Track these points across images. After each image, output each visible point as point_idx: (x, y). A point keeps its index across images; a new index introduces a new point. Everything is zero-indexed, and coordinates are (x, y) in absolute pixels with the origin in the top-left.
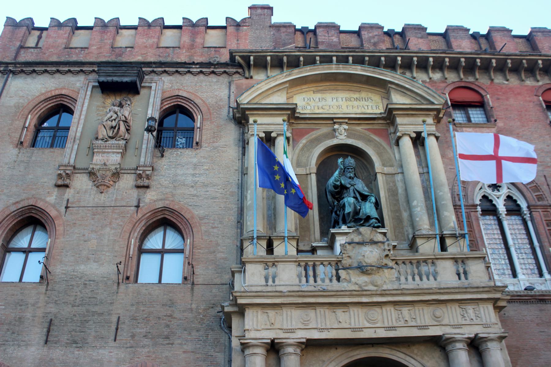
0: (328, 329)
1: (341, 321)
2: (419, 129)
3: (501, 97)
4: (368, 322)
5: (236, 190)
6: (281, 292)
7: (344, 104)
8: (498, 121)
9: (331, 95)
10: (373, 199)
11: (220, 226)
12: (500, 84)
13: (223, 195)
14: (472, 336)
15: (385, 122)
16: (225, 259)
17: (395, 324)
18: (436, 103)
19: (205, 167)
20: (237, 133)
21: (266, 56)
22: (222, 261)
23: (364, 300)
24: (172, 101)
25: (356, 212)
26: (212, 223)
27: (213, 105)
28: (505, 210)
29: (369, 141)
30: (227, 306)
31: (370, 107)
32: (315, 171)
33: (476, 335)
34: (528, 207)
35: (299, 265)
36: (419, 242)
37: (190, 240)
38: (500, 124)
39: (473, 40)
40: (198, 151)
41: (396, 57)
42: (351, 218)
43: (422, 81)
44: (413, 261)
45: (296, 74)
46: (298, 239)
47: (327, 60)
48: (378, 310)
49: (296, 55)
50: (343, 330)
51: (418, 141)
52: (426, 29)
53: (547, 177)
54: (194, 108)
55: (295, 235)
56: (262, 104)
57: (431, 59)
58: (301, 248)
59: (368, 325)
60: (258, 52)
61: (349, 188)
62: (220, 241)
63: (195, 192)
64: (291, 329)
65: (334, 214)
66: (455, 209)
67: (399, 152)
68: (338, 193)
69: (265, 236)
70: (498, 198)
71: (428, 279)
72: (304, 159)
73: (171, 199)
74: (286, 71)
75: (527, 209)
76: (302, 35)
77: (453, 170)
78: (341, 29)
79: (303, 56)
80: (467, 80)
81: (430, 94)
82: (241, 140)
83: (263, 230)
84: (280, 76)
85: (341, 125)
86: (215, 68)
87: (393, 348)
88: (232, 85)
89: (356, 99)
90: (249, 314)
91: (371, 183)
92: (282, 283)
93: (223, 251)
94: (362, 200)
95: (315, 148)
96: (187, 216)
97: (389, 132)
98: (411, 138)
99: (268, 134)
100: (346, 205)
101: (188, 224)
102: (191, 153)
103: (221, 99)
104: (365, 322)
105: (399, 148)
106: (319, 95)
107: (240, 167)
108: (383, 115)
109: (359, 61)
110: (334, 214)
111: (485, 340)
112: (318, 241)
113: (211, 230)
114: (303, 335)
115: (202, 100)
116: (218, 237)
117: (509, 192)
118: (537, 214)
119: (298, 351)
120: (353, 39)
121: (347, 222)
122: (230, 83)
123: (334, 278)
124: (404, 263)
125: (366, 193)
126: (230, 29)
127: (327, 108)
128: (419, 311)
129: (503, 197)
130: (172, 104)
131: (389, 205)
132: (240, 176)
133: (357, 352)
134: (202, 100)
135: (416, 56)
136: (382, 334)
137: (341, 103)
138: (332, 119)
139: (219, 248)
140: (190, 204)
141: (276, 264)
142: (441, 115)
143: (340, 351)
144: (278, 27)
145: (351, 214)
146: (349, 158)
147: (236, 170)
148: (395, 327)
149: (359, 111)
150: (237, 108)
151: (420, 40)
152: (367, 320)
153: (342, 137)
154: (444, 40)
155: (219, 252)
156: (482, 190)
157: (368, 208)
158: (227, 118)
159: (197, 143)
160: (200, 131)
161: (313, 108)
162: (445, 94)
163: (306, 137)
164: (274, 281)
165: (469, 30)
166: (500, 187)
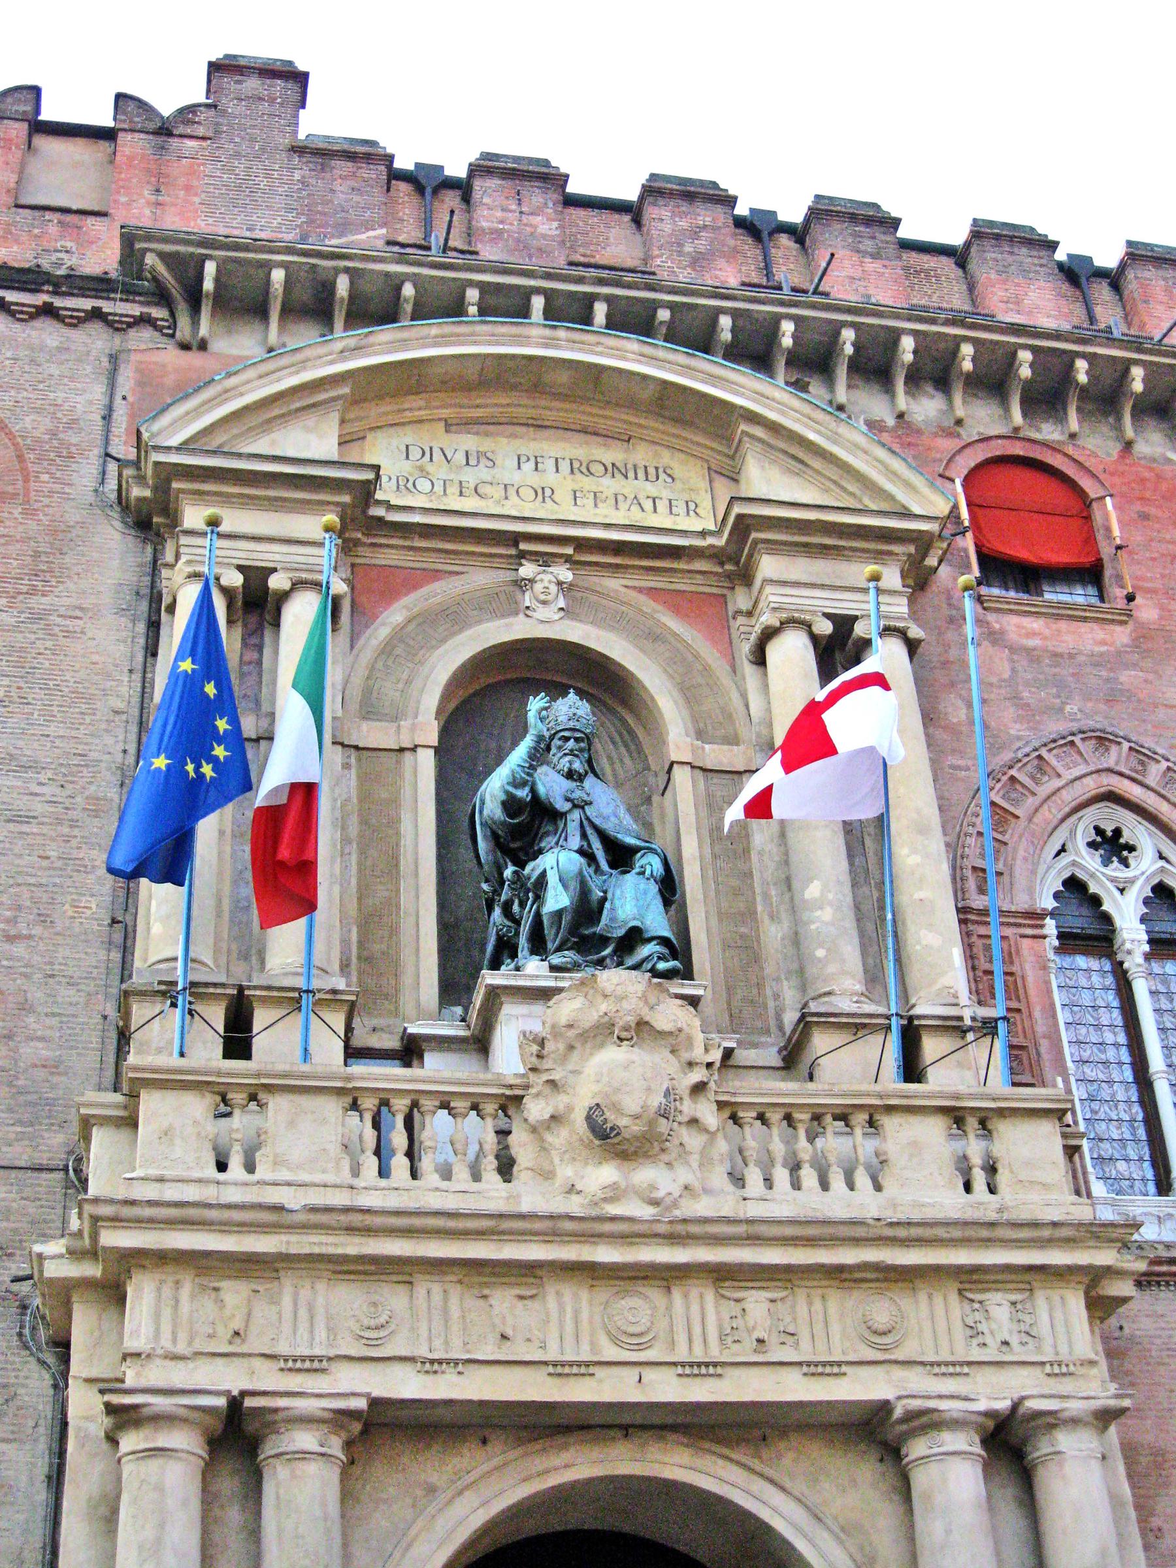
0: (456, 1362)
1: (509, 1332)
2: (845, 605)
3: (1153, 511)
4: (616, 1341)
5: (113, 794)
6: (279, 1208)
8: (1139, 600)
9: (518, 442)
10: (654, 864)
11: (37, 931)
12: (1153, 460)
13: (60, 809)
14: (1003, 1405)
16: (53, 1067)
17: (715, 1354)
20: (131, 560)
21: (268, 266)
22: (41, 1074)
23: (605, 1254)
25: (587, 910)
27: (37, 441)
30: (53, 1257)
31: (662, 506)
32: (432, 736)
33: (1015, 1406)
35: (355, 1106)
36: (821, 1041)
38: (1146, 611)
39: (1065, 287)
41: (777, 319)
44: (797, 1116)
45: (386, 347)
46: (353, 1004)
47: (507, 305)
48: (655, 1294)
49: (387, 275)
50: (518, 1371)
52: (895, 223)
55: (341, 985)
56: (239, 455)
57: (907, 344)
58: (362, 1039)
59: (611, 1353)
60: (237, 247)
61: (563, 815)
62: (37, 995)
64: (312, 1359)
65: (497, 912)
68: (516, 832)
69: (223, 985)
70: (1122, 891)
71: (851, 1186)
72: (389, 690)
74: (342, 337)
76: (415, 199)
78: (571, 188)
79: (416, 280)
81: (895, 474)
84: (321, 351)
86: (55, 293)
87: (707, 1445)
89: (613, 470)
90: (143, 1293)
91: (648, 800)
92: (285, 1175)
93: (48, 1033)
94: (613, 865)
97: (731, 609)
98: (814, 639)
99: (256, 576)
103: (75, 421)
104: (604, 1341)
105: (765, 674)
106: (468, 442)
107: (136, 700)
108: (710, 541)
109: (633, 321)
110: (497, 912)
111: (1051, 1421)
114: (358, 1385)
117: (1162, 870)
119: (335, 1446)
120: (614, 233)
121: (551, 946)
122: (114, 359)
123: (490, 1164)
124: (761, 1117)
125: (631, 841)
126: (131, 145)
127: (498, 492)
128: (810, 1304)
129: (1139, 891)
132: (133, 737)
133: (565, 1457)
135: (853, 325)
136: (667, 1389)
137: (550, 478)
138: (515, 539)
141: (262, 1096)
142: (931, 561)
143: (497, 1453)
144: (322, 154)
146: (572, 695)
148: (715, 1365)
149: (620, 518)
150: (137, 464)
151: (871, 265)
152: (609, 1333)
153: (544, 618)
154: (960, 272)
156: (1065, 859)
158: (91, 498)
161: (439, 488)
162: (953, 481)
163: (407, 600)
164: (250, 1167)
165: (1053, 246)
166: (1132, 849)
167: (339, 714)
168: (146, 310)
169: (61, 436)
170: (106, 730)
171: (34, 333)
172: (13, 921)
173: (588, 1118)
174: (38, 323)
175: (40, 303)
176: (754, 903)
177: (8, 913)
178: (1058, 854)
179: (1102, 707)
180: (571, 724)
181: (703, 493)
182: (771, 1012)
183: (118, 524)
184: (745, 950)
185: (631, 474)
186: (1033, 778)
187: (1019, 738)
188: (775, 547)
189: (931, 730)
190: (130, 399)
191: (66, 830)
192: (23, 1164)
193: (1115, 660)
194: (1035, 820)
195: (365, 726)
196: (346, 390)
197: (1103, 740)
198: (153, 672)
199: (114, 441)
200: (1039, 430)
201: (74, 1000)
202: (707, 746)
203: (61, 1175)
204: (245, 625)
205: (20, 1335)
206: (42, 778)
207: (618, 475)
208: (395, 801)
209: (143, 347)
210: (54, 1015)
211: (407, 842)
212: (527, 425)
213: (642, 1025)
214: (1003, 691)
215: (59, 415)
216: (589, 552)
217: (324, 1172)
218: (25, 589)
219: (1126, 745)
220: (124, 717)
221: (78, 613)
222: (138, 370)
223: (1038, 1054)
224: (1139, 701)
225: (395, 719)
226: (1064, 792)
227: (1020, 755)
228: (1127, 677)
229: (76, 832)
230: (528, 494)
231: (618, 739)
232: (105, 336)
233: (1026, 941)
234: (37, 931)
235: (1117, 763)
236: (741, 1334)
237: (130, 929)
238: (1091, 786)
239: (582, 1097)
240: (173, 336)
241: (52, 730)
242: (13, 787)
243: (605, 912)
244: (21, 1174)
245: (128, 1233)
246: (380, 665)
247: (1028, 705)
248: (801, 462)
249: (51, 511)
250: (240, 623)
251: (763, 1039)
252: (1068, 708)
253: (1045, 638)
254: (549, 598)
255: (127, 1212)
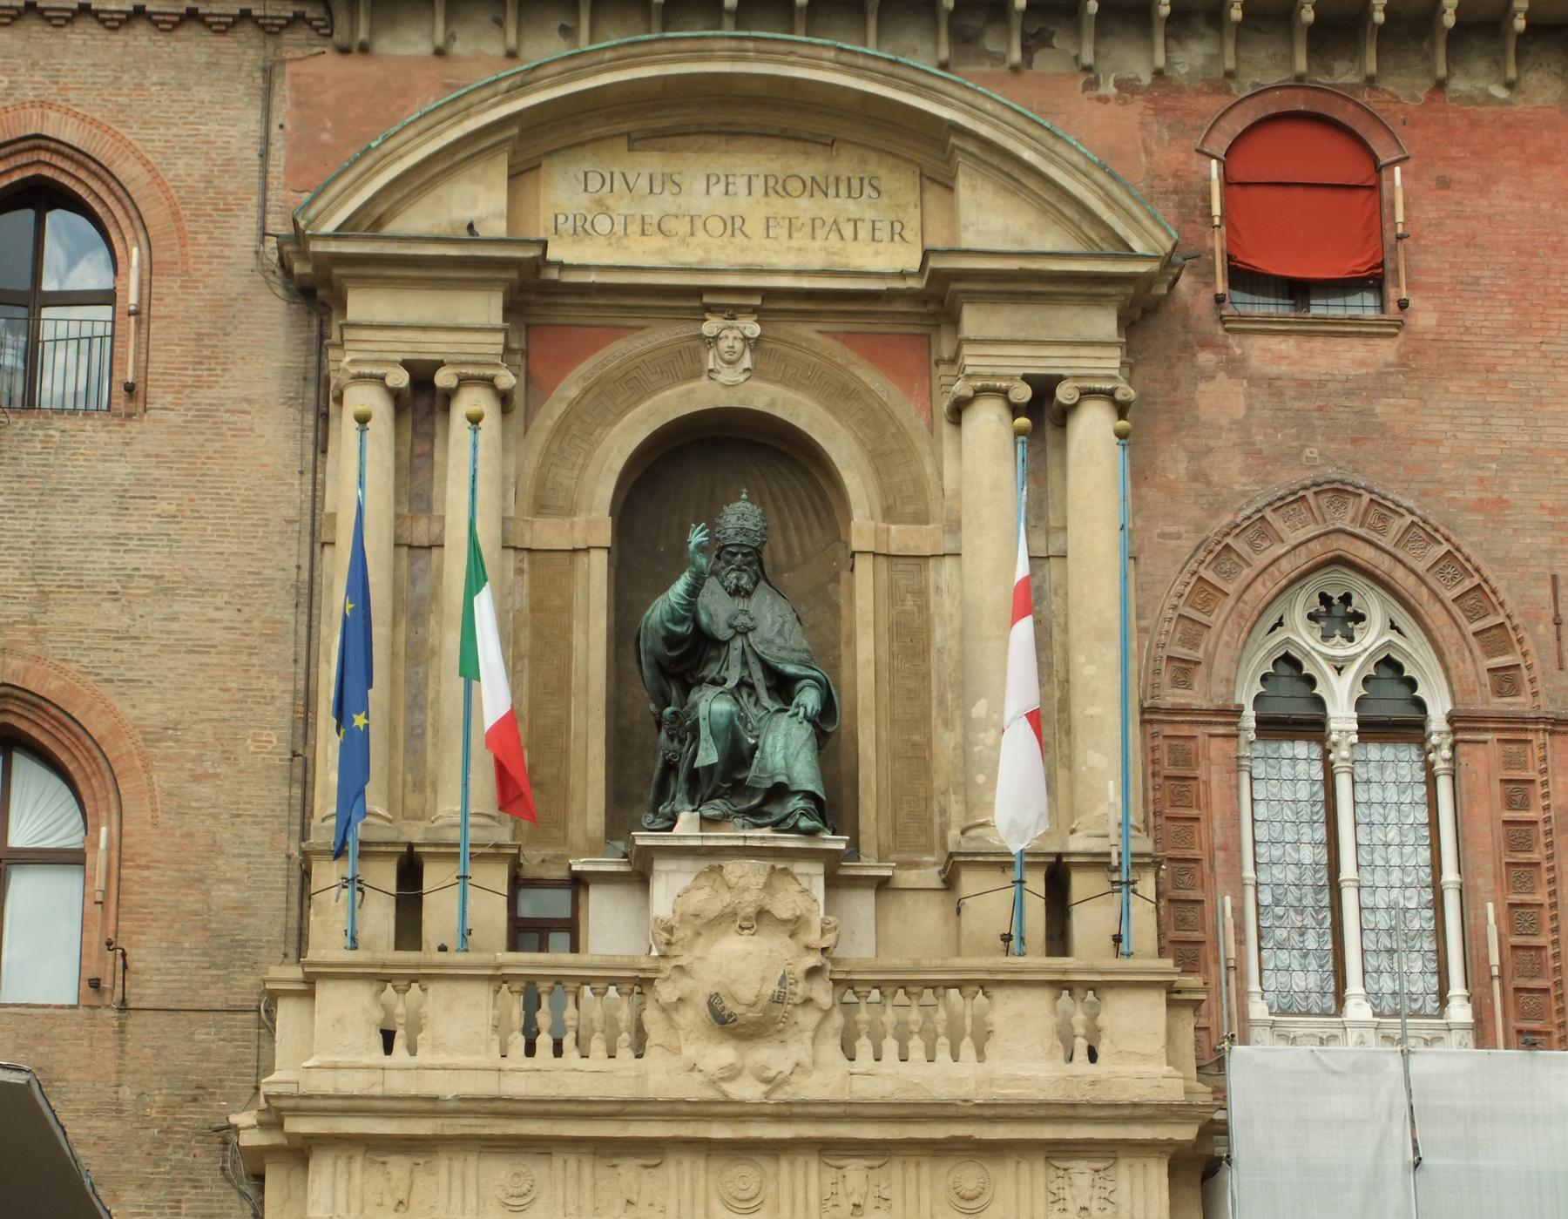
1: (634, 1198)
3: (1458, 174)
7: (751, 206)
10: (809, 699)
11: (222, 769)
12: (1470, 99)
15: (922, 310)
16: (243, 908)
18: (1138, 246)
19: (164, 505)
23: (719, 1131)
24: (13, 162)
26: (193, 760)
27: (193, 190)
28: (1356, 727)
29: (841, 394)
32: (604, 534)
34: (1452, 719)
36: (970, 882)
37: (109, 825)
38: (1424, 317)
40: (134, 427)
42: (716, 781)
43: (1120, 84)
51: (1043, 412)
53: (1562, 583)
54: (110, 201)
61: (726, 643)
63: (126, 620)
65: (663, 735)
66: (1143, 722)
67: (959, 453)
68: (678, 661)
69: (394, 844)
70: (1339, 670)
73: (30, 650)
75: (1445, 727)
77: (1172, 543)
80: (1325, 80)
81: (1115, 201)
82: (313, 374)
83: (390, 810)
85: (733, 318)
88: (278, 82)
89: (815, 187)
92: (441, 1059)
93: (236, 874)
95: (613, 424)
96: (97, 726)
100: (704, 732)
101: (101, 759)
102: (102, 436)
103: (229, 162)
106: (650, 163)
107: (308, 505)
108: (912, 283)
112: (594, 853)
113: (194, 787)
115: (146, 163)
116: (215, 817)
117: (1389, 644)
118: (1479, 751)
122: (268, 74)
125: (791, 669)
127: (681, 227)
128: (904, 1170)
130: (16, 177)
131: (885, 700)
132: (306, 549)
134: (146, 163)
137: (742, 203)
138: (699, 291)
139: (220, 862)
140: (106, 674)
145: (721, 767)
147: (290, 522)
153: (728, 380)
155: (222, 881)
156: (1280, 635)
157: (786, 749)
158: (251, 262)
159: (130, 389)
160: (139, 323)
161: (619, 228)
164: (412, 1050)
166: (1359, 618)
167: (512, 513)
168: (298, 8)
169: (217, 182)
170: (281, 544)
171: (179, 46)
172: (199, 759)
173: (710, 1004)
174: (182, 33)
175: (183, 10)
176: (928, 708)
177: (194, 752)
178: (1273, 629)
179: (1349, 447)
180: (738, 540)
181: (911, 209)
182: (936, 829)
183: (280, 291)
184: (914, 759)
185: (832, 191)
186: (1251, 544)
187: (1243, 494)
188: (977, 298)
189: (1144, 491)
190: (288, 127)
191: (244, 658)
192: (217, 1006)
193: (1379, 384)
194: (1246, 597)
195: (539, 523)
196: (515, 131)
197: (1340, 491)
198: (324, 472)
199: (270, 219)
200: (1330, 72)
201: (259, 839)
202: (893, 527)
203: (252, 1016)
204: (415, 411)
205: (223, 1169)
206: (219, 601)
207: (817, 193)
208: (567, 609)
209: (299, 53)
210: (241, 856)
211: (578, 655)
212: (719, 133)
213: (762, 914)
214: (1234, 436)
215: (213, 155)
216: (777, 304)
217: (477, 1053)
218: (189, 381)
219: (1366, 497)
220: (297, 527)
221: (245, 406)
222: (296, 88)
223: (1212, 867)
224: (1394, 437)
225: (571, 512)
226: (1284, 562)
227: (1238, 520)
228: (1384, 408)
229: (254, 660)
230: (715, 225)
231: (808, 504)
232: (255, 41)
233: (1214, 741)
234: (222, 769)
235: (1353, 520)
236: (842, 1200)
237: (310, 762)
238: (1318, 550)
239: (701, 985)
240: (331, 35)
241: (227, 546)
242: (192, 614)
243: (755, 762)
244: (218, 1016)
245: (307, 1120)
246: (555, 448)
247: (1260, 452)
248: (1016, 180)
249: (210, 281)
250: (410, 410)
251: (926, 858)
252: (1307, 451)
253: (1294, 363)
254: (734, 357)
255: (304, 1103)
